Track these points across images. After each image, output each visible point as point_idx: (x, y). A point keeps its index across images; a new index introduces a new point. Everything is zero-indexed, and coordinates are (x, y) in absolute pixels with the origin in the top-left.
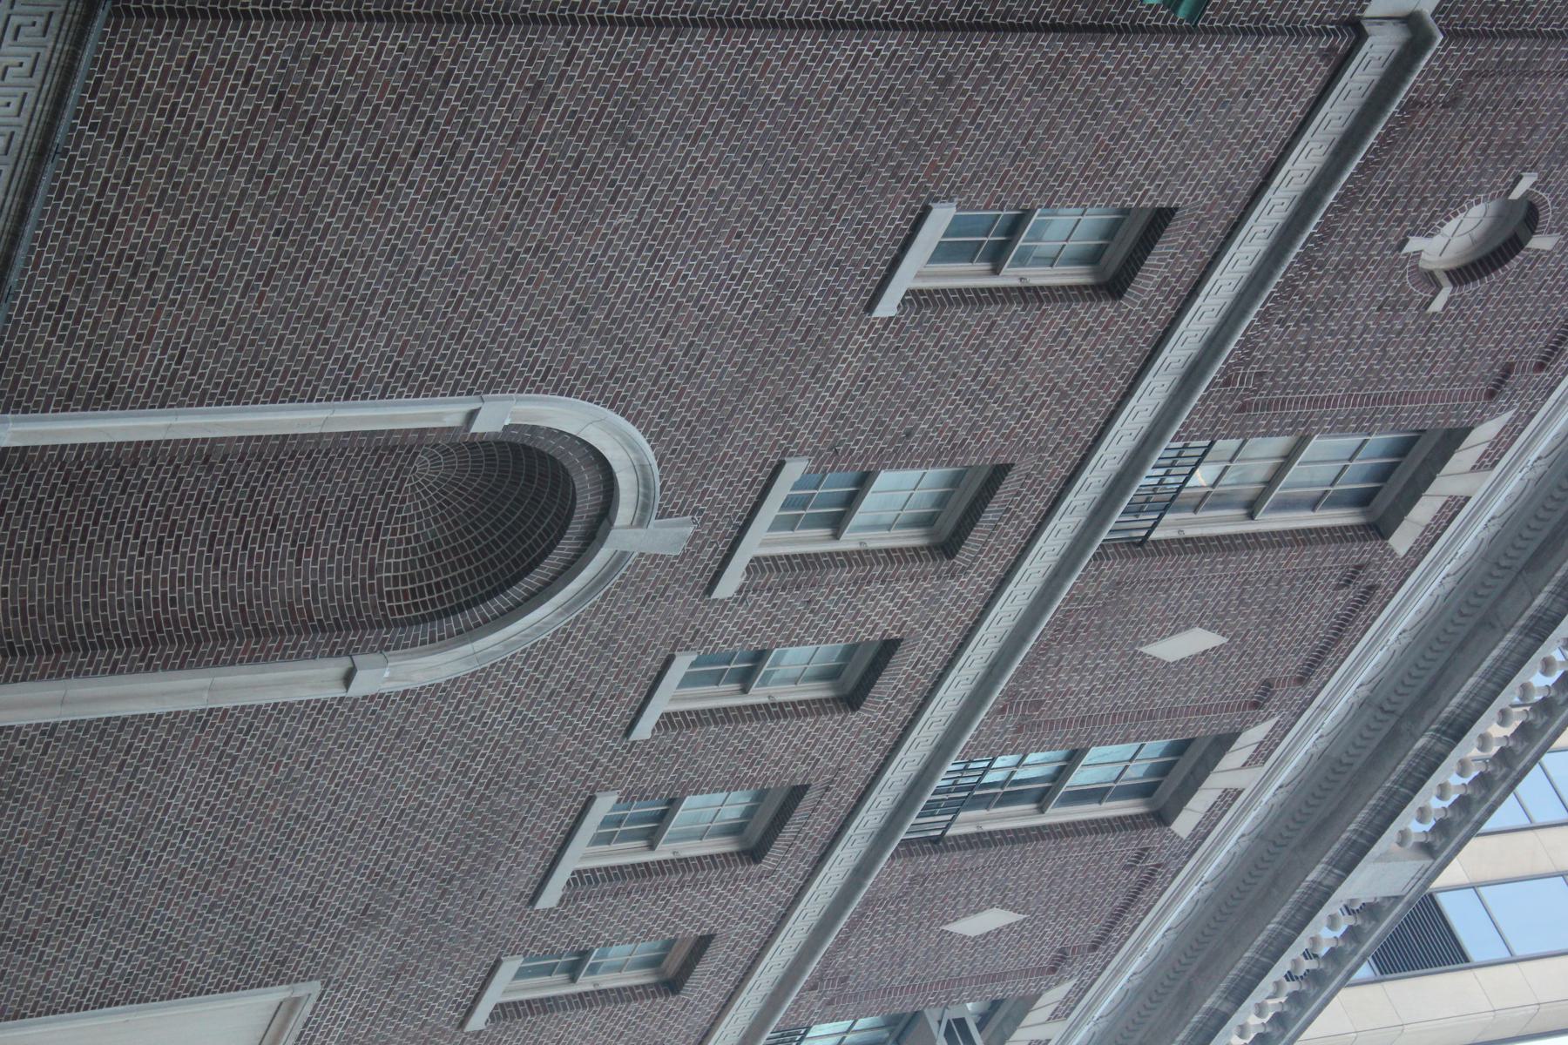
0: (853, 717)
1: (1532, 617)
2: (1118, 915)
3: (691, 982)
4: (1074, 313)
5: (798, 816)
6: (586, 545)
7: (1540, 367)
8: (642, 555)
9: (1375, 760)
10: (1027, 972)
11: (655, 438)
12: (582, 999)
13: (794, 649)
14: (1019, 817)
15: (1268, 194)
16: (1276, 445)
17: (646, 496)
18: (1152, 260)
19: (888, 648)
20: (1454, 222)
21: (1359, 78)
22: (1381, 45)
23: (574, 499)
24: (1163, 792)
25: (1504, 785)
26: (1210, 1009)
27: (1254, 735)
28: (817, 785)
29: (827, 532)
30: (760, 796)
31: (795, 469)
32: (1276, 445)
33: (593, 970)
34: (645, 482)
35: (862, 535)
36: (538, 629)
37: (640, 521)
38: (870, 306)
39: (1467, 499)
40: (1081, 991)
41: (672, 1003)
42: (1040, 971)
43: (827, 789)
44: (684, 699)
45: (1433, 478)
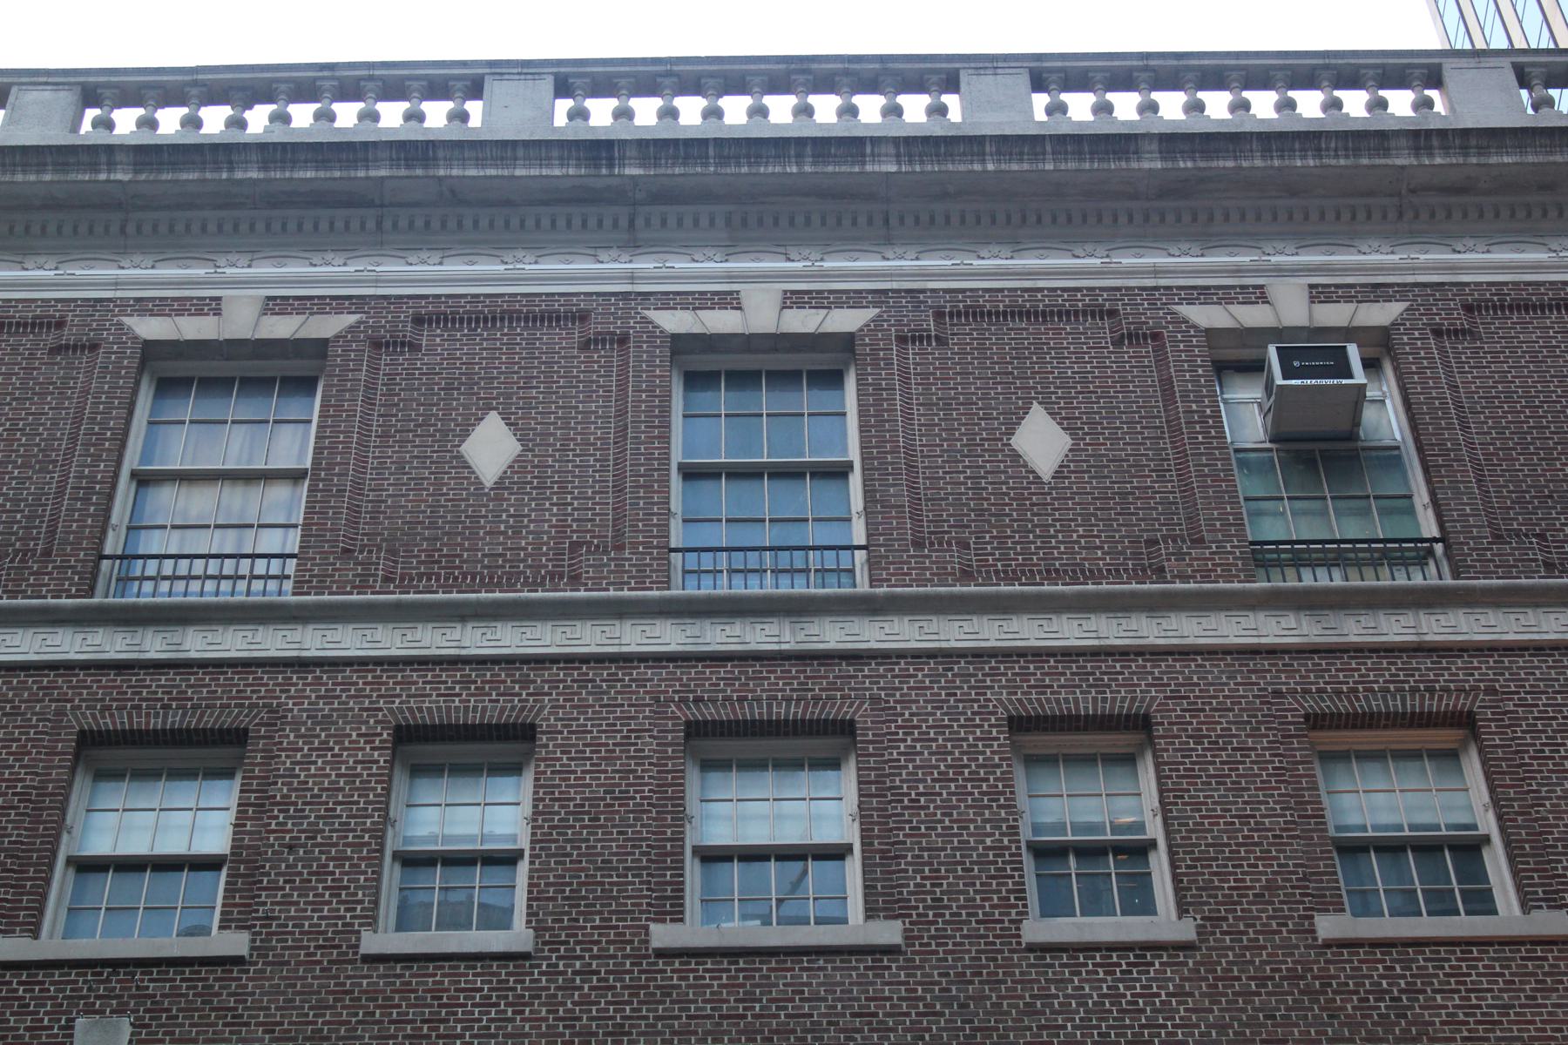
1: (408, 167)
9: (704, 196)
26: (1163, 159)
28: (694, 713)
39: (269, 298)
43: (697, 700)
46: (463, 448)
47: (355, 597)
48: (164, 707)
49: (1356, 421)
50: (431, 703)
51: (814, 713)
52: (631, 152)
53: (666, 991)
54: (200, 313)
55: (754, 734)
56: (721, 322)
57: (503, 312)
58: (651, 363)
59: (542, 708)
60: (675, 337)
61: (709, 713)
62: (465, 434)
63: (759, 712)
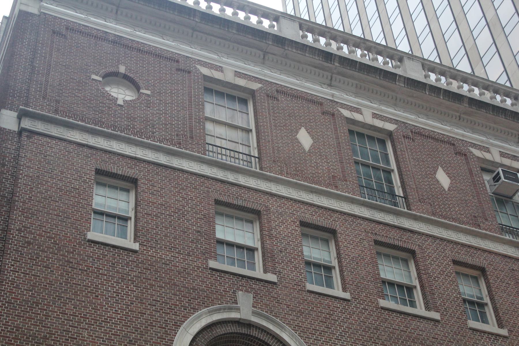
0: (339, 231)
2: (437, 140)
3: (478, 264)
4: (143, 191)
5: (383, 240)
6: (253, 326)
7: (178, 61)
8: (253, 307)
10: (468, 163)
11: (195, 310)
12: (492, 299)
13: (304, 253)
14: (396, 178)
15: (91, 144)
16: (209, 126)
17: (225, 309)
18: (120, 172)
19: (303, 224)
20: (112, 94)
21: (40, 127)
22: (27, 124)
23: (232, 333)
24: (381, 138)
25: (332, 31)
27: (346, 113)
28: (374, 237)
29: (256, 253)
30: (379, 254)
31: (212, 264)
32: (209, 126)
33: (481, 298)
34: (218, 310)
35: (256, 240)
36: (292, 336)
37: (238, 310)
38: (135, 252)
39: (236, 71)
40: (474, 146)
41: (489, 270)
42: (466, 159)
43: (376, 234)
44: (338, 286)
45: (227, 82)
46: (298, 136)
47: (280, 176)
48: (236, 198)
49: (514, 195)
50: (309, 217)
51: (405, 245)
52: (402, 79)
53: (386, 320)
54: (216, 70)
55: (388, 247)
56: (357, 117)
57: (300, 96)
58: (342, 124)
59: (337, 226)
60: (347, 118)
61: (379, 238)
62: (297, 132)
63: (391, 242)
